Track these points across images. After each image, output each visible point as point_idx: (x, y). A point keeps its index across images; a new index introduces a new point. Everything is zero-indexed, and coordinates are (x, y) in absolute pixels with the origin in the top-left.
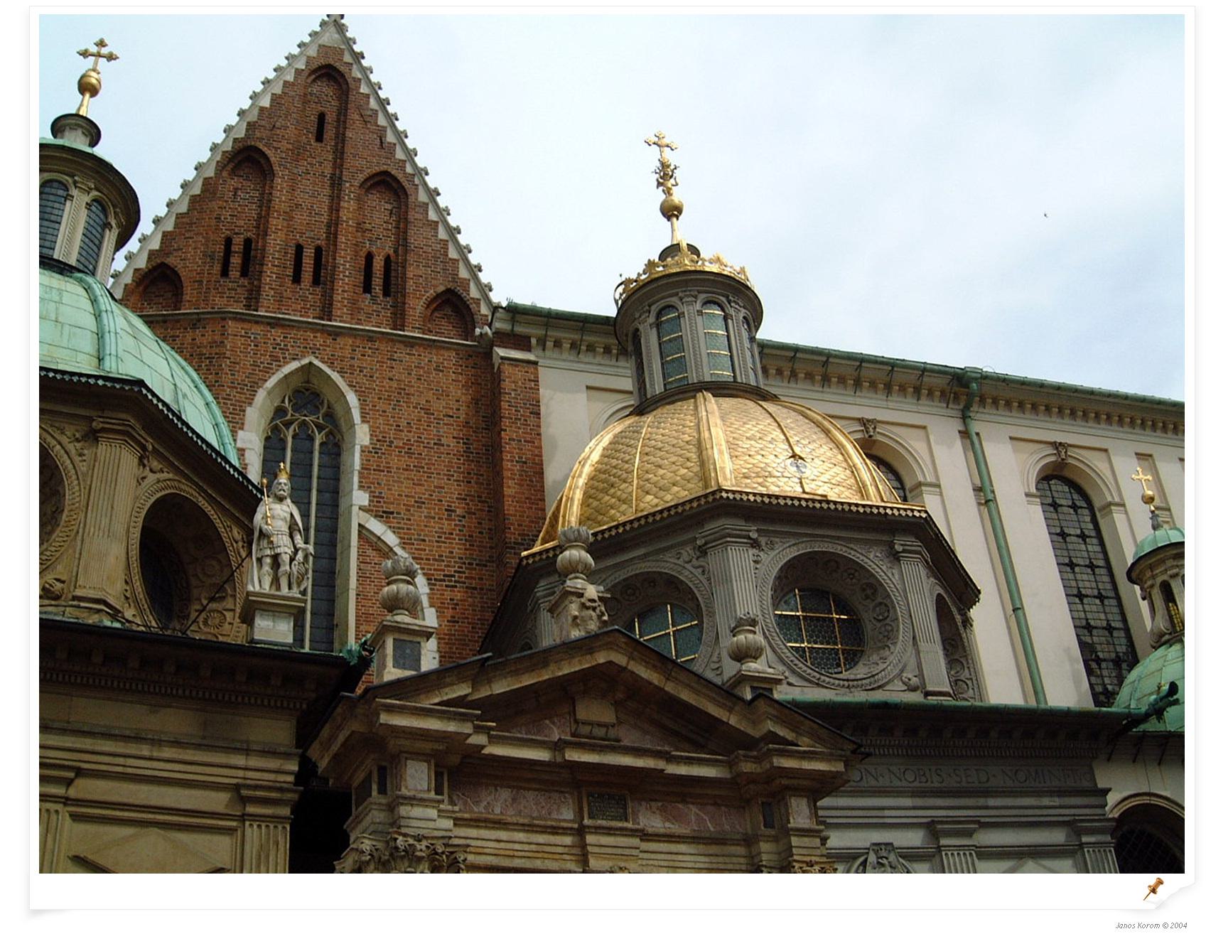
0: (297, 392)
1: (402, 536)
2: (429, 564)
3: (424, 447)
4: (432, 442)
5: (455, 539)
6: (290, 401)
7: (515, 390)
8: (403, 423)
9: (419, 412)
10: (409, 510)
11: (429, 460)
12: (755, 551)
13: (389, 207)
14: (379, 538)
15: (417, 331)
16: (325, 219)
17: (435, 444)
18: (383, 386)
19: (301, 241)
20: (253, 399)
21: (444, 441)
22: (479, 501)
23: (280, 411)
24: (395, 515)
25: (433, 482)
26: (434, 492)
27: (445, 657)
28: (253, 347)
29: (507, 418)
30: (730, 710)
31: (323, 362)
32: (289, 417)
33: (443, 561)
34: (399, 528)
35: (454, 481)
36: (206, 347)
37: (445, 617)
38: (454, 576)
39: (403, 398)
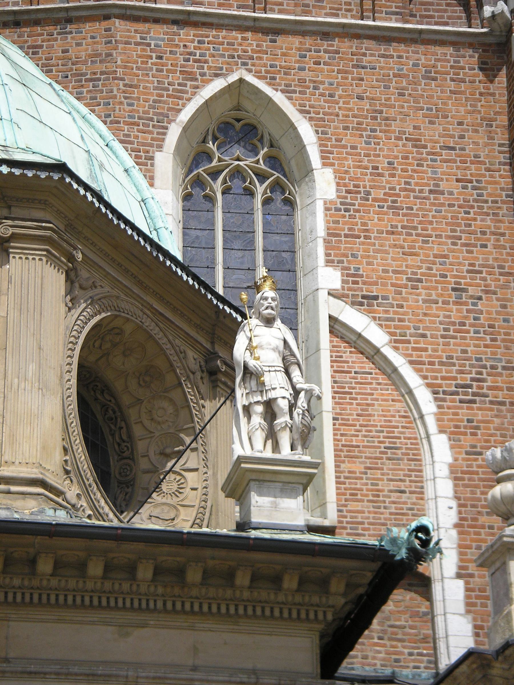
1: (393, 330)
2: (433, 371)
3: (415, 197)
4: (427, 188)
5: (468, 332)
9: (404, 145)
10: (400, 293)
11: (424, 216)
14: (360, 335)
15: (393, 17)
17: (431, 192)
18: (350, 109)
20: (163, 140)
21: (443, 186)
22: (501, 274)
24: (380, 300)
25: (432, 249)
26: (434, 263)
27: (464, 506)
28: (154, 60)
31: (259, 78)
32: (214, 163)
33: (454, 365)
34: (387, 319)
35: (463, 245)
36: (85, 62)
37: (460, 447)
38: (470, 386)
39: (380, 125)
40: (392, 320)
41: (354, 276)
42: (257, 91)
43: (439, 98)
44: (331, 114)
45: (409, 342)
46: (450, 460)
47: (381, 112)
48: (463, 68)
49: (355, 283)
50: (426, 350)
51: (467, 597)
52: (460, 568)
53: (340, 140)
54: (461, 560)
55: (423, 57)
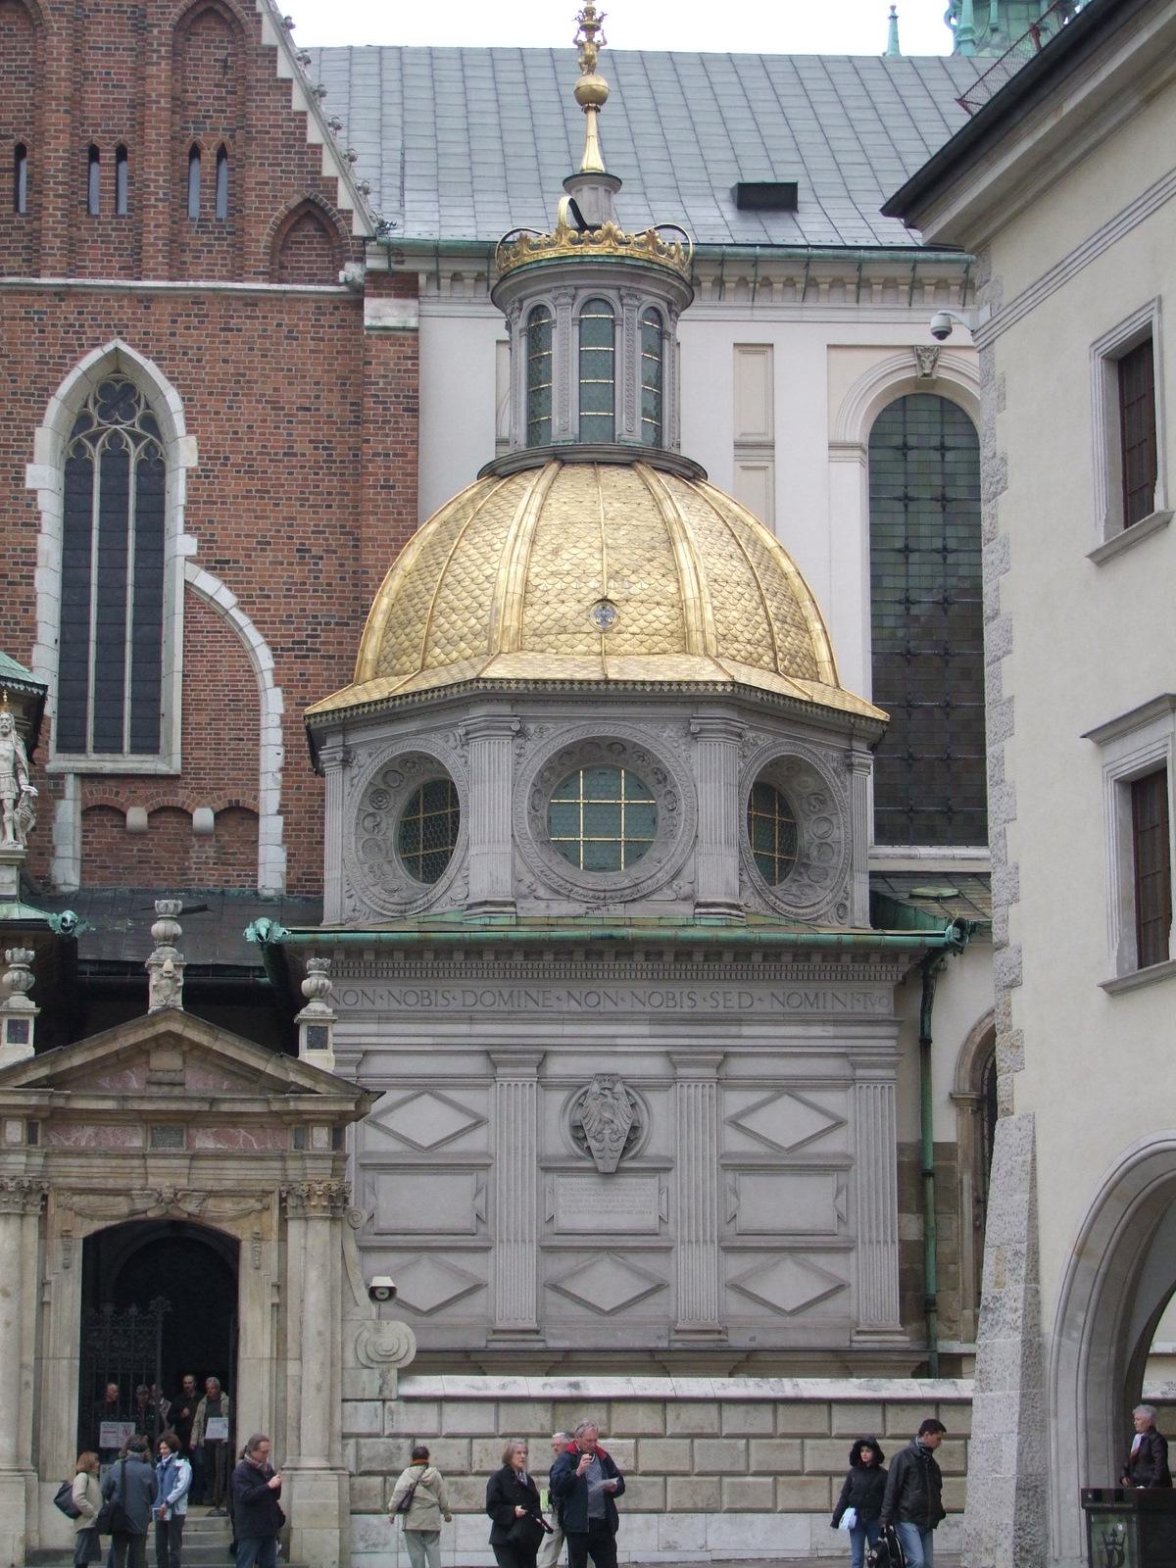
0: (105, 389)
6: (96, 402)
7: (385, 376)
8: (243, 429)
10: (250, 556)
12: (520, 741)
13: (221, 54)
16: (126, 95)
17: (285, 454)
18: (215, 374)
19: (96, 140)
22: (342, 533)
23: (83, 421)
26: (283, 525)
29: (372, 422)
30: (268, 1061)
31: (133, 346)
34: (236, 582)
35: (310, 506)
38: (306, 643)
40: (242, 582)
41: (209, 541)
42: (130, 358)
43: (299, 358)
44: (198, 380)
45: (254, 603)
46: (282, 711)
47: (244, 375)
48: (323, 326)
49: (210, 548)
50: (269, 610)
51: (285, 830)
52: (281, 806)
53: (205, 406)
54: (283, 799)
55: (286, 317)
